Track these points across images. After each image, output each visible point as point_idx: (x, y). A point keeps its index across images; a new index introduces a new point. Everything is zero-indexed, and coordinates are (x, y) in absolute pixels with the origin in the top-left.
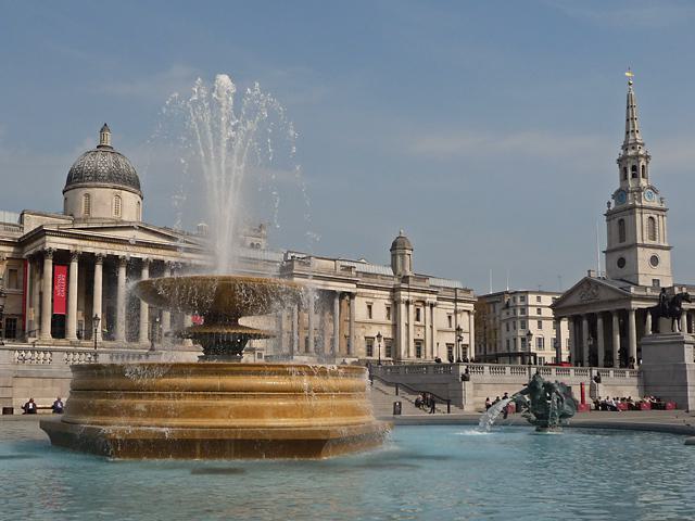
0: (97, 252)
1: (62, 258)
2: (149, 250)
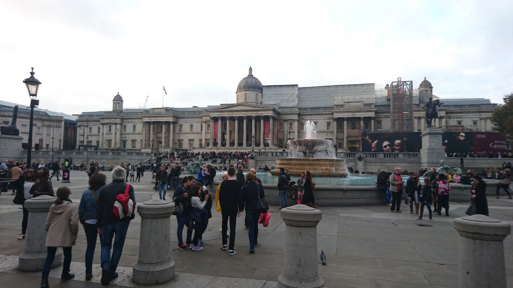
0: (226, 116)
1: (215, 119)
2: (246, 113)
